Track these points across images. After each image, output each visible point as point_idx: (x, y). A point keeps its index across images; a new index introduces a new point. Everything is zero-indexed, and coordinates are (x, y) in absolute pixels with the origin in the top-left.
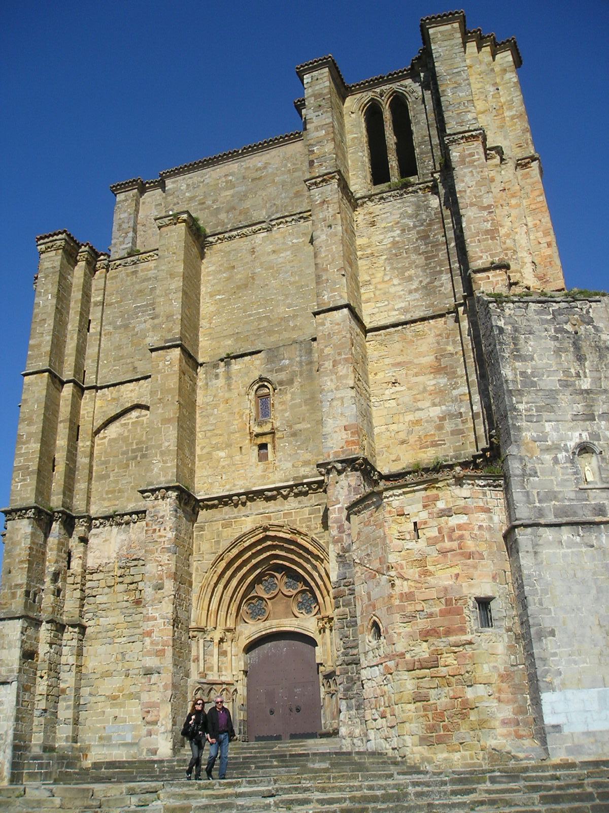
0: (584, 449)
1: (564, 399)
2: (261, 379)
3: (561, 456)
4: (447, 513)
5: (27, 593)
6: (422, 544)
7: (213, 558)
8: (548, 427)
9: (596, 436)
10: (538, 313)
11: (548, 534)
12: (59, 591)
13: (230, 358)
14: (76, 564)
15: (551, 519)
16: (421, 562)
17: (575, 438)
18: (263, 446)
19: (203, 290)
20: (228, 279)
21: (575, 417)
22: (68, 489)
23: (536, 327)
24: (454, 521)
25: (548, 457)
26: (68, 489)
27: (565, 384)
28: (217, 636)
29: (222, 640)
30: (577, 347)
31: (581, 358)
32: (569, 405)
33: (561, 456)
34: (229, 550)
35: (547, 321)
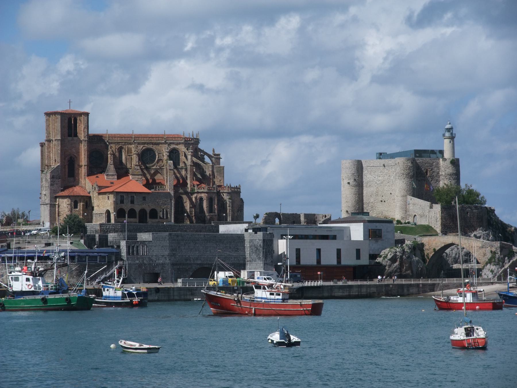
17: (45, 193)
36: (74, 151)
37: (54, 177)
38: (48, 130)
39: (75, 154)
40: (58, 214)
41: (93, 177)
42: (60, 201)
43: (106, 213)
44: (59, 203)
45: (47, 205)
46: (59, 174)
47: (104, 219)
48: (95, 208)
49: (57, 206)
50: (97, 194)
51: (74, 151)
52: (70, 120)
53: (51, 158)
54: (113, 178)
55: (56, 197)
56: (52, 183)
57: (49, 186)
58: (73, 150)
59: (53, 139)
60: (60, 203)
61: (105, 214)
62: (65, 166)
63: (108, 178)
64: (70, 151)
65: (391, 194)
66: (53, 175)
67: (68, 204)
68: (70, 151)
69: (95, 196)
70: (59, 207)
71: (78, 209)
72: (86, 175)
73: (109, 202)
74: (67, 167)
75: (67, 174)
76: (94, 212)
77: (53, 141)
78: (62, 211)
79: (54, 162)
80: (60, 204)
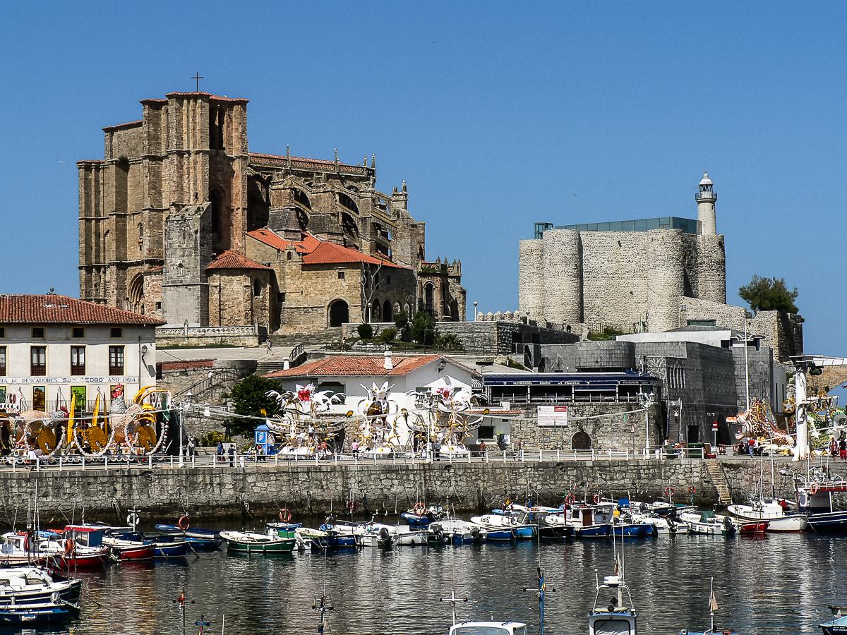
0: (181, 266)
1: (178, 251)
2: (140, 223)
3: (175, 267)
4: (153, 281)
5: (86, 292)
6: (149, 288)
7: (130, 281)
8: (173, 259)
9: (183, 261)
10: (176, 224)
11: (169, 288)
12: (97, 290)
13: (134, 214)
14: (102, 280)
15: (170, 284)
16: (149, 293)
18: (141, 246)
19: (128, 184)
20: (134, 181)
21: (180, 256)
22: (97, 256)
23: (175, 228)
24: (155, 283)
25: (172, 268)
26: (97, 256)
27: (179, 246)
28: (134, 303)
29: (136, 305)
30: (184, 235)
31: (184, 238)
32: (179, 253)
33: (175, 267)
34: (134, 279)
35: (178, 227)
36: (220, 178)
41: (257, 233)
43: (329, 306)
45: (190, 287)
47: (325, 319)
50: (294, 266)
51: (220, 178)
53: (186, 189)
54: (294, 237)
57: (196, 248)
59: (191, 150)
61: (328, 309)
63: (288, 237)
65: (631, 293)
67: (245, 286)
69: (287, 270)
71: (261, 297)
73: (344, 284)
76: (286, 304)
78: (228, 301)
79: (192, 198)
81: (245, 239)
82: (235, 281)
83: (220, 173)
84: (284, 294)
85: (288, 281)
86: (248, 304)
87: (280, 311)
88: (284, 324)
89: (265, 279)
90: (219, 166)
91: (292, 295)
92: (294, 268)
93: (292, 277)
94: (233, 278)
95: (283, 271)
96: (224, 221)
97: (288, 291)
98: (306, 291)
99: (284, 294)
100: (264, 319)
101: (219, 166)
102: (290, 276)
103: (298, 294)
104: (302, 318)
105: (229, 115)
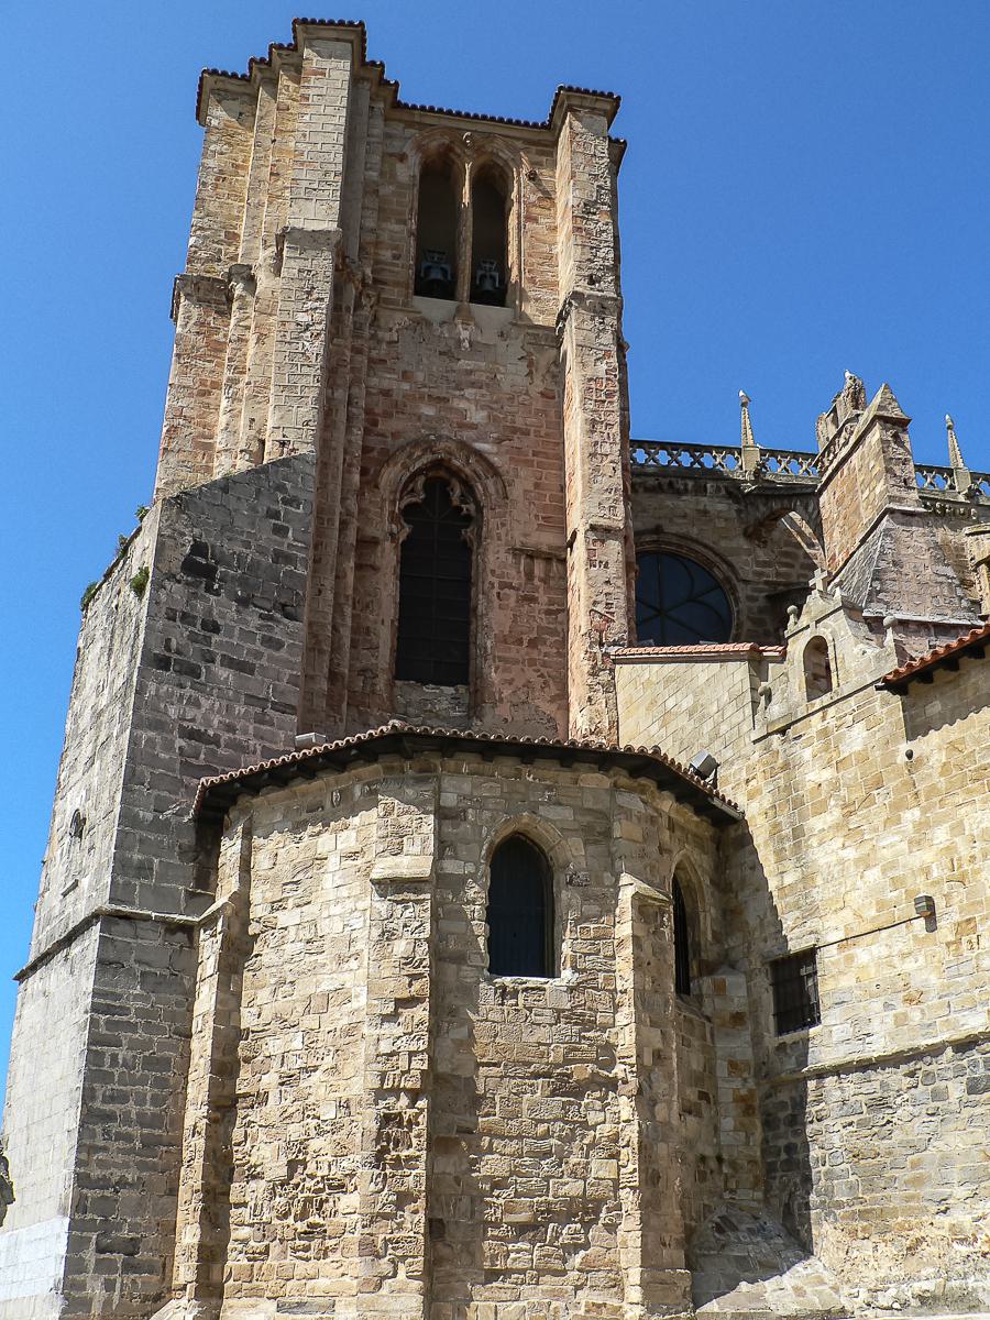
37: (208, 573)
38: (212, 207)
39: (479, 446)
40: (226, 1067)
42: (261, 861)
44: (242, 901)
46: (289, 559)
48: (833, 981)
49: (209, 949)
51: (477, 416)
52: (437, 176)
55: (213, 816)
56: (179, 635)
58: (463, 405)
60: (256, 895)
62: (366, 544)
64: (428, 410)
66: (199, 548)
67: (390, 887)
68: (428, 410)
70: (237, 953)
71: (567, 975)
72: (619, 626)
74: (388, 557)
75: (385, 637)
76: (829, 1042)
77: (251, 281)
78: (285, 1024)
80: (257, 911)
81: (610, 687)
82: (333, 862)
83: (469, 392)
84: (809, 955)
85: (827, 853)
86: (408, 1036)
87: (800, 1103)
88: (829, 1208)
89: (598, 832)
90: (464, 364)
91: (863, 954)
92: (856, 739)
93: (849, 810)
94: (325, 842)
95: (791, 798)
96: (495, 617)
97: (832, 928)
98: (960, 895)
99: (809, 955)
100: (601, 1168)
101: (464, 364)
102: (834, 815)
103: (899, 940)
104: (955, 1141)
105: (532, 177)
